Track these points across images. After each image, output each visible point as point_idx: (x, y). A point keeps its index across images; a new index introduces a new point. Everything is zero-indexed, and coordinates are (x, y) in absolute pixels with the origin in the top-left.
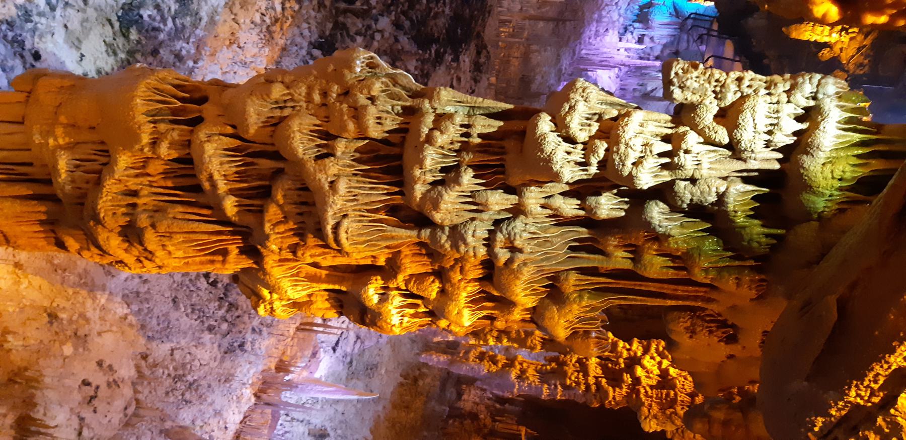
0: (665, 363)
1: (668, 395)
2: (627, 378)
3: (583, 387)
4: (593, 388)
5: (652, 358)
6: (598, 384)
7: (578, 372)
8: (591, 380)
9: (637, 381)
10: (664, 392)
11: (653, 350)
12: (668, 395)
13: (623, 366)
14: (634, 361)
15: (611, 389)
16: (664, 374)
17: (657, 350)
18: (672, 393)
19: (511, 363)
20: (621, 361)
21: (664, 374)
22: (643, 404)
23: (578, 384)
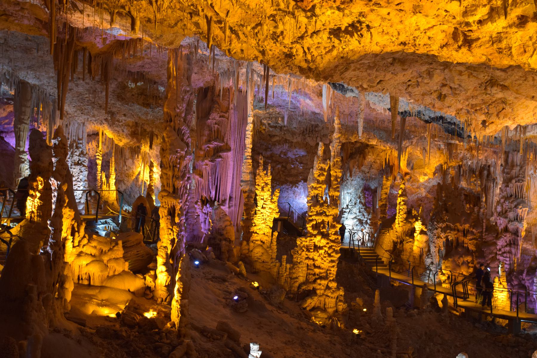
0: (326, 249)
1: (311, 249)
2: (315, 232)
3: (311, 214)
4: (310, 218)
5: (328, 243)
6: (312, 220)
7: (317, 212)
8: (313, 217)
9: (315, 236)
10: (313, 248)
11: (332, 244)
12: (311, 249)
13: (322, 231)
14: (325, 236)
15: (310, 225)
16: (321, 248)
17: (333, 246)
18: (312, 251)
19: (318, 182)
20: (324, 230)
21: (321, 248)
22: (306, 238)
23: (312, 212)
